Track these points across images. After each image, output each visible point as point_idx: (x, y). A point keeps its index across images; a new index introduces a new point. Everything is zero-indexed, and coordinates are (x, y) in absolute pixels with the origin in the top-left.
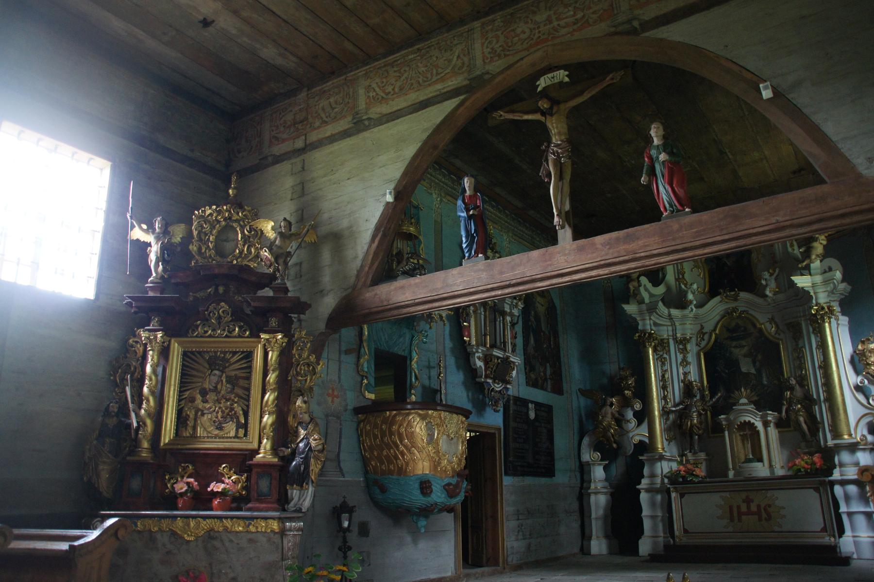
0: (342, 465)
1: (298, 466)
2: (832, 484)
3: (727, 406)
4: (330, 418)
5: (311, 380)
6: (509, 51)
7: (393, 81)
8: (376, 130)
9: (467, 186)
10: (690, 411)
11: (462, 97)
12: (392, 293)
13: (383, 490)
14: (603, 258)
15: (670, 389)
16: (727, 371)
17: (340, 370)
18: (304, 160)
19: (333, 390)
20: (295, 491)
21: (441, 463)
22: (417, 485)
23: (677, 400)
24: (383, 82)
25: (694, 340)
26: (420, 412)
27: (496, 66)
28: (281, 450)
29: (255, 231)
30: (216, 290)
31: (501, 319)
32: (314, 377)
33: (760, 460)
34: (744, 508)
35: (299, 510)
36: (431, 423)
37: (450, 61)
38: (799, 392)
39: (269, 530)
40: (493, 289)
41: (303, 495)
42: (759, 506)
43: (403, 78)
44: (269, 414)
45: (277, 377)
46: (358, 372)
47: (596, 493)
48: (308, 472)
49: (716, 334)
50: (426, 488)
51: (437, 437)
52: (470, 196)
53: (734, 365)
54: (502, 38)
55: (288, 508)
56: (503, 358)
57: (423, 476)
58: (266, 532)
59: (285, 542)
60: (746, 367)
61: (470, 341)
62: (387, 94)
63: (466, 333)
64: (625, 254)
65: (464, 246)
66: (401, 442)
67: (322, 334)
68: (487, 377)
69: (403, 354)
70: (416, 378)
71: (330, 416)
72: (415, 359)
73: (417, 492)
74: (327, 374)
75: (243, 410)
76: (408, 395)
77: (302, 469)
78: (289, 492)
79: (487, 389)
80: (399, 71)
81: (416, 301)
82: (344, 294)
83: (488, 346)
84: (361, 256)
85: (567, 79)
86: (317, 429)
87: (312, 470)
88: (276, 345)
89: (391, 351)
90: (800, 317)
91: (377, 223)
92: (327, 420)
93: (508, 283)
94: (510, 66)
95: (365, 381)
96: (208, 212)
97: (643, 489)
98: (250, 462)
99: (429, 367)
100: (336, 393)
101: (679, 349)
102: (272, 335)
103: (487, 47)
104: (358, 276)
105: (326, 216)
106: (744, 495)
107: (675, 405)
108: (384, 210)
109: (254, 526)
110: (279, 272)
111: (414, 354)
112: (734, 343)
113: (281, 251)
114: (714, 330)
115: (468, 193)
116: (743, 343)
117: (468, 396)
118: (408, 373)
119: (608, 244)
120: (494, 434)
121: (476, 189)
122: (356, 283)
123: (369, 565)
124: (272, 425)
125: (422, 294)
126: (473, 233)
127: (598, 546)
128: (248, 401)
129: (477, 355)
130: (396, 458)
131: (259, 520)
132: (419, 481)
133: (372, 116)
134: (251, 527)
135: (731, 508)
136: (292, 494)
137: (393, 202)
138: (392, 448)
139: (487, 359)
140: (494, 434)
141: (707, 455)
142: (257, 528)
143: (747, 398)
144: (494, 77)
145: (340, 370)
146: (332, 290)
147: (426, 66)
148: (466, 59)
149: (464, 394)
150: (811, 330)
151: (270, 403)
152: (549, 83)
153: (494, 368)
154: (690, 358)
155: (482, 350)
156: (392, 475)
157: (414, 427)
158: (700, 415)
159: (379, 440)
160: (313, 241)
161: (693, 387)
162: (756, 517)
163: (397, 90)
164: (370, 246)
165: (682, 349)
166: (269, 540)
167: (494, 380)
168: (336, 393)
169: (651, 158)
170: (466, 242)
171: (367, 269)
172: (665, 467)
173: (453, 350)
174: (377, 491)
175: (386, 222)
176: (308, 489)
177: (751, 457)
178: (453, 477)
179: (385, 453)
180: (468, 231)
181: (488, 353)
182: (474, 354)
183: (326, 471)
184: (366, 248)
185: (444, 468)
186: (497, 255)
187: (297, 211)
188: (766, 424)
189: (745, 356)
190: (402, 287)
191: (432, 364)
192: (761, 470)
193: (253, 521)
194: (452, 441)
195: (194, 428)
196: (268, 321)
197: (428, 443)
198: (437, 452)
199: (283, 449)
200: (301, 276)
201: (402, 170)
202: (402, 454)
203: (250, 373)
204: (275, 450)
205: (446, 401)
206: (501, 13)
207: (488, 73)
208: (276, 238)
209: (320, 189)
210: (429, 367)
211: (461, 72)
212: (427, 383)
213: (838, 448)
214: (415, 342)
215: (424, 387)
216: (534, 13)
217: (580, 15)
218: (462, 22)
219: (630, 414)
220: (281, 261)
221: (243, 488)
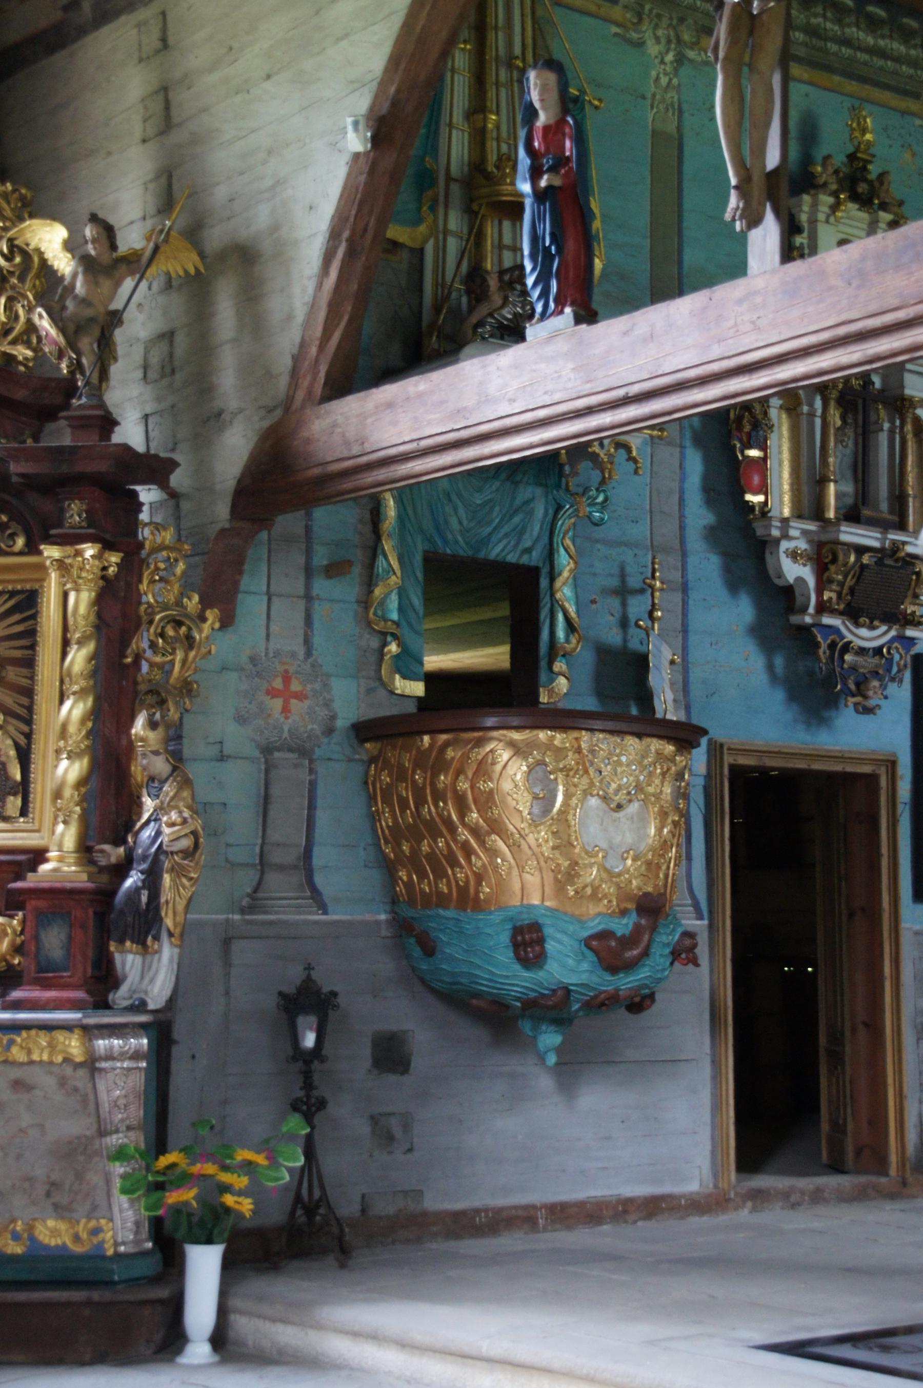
0: (319, 880)
1: (135, 891)
4: (277, 755)
5: (184, 662)
9: (535, 96)
12: (369, 421)
13: (429, 948)
14: (844, 317)
17: (308, 620)
18: (164, 14)
19: (287, 679)
20: (130, 957)
21: (578, 875)
22: (505, 937)
26: (516, 736)
28: (102, 851)
29: (26, 255)
31: (898, 423)
32: (192, 654)
35: (140, 1007)
36: (546, 765)
39: (60, 1059)
40: (589, 411)
41: (150, 967)
44: (69, 758)
45: (93, 657)
46: (369, 624)
48: (157, 909)
50: (532, 943)
51: (565, 803)
52: (546, 129)
55: (114, 1003)
56: (881, 550)
57: (521, 913)
58: (51, 1063)
59: (101, 1086)
61: (766, 503)
63: (756, 479)
64: (895, 302)
65: (530, 281)
66: (462, 815)
67: (223, 531)
68: (822, 608)
69: (525, 560)
70: (571, 627)
71: (278, 749)
72: (566, 574)
73: (505, 956)
75: (17, 746)
76: (543, 676)
77: (144, 898)
78: (118, 957)
79: (824, 646)
81: (424, 443)
82: (266, 424)
83: (831, 514)
84: (300, 315)
86: (186, 794)
87: (167, 902)
88: (84, 574)
89: (482, 555)
91: (333, 217)
92: (266, 762)
93: (621, 393)
95: (393, 648)
98: (19, 885)
99: (623, 592)
100: (295, 686)
102: (69, 550)
104: (295, 372)
105: (221, 193)
108: (349, 175)
109: (21, 1047)
110: (83, 373)
111: (562, 559)
113: (89, 312)
115: (542, 119)
117: (770, 668)
118: (544, 613)
120: (872, 779)
122: (291, 393)
123: (410, 1150)
124: (81, 783)
126: (547, 244)
128: (29, 722)
129: (784, 545)
130: (453, 862)
131: (33, 1032)
132: (509, 926)
134: (15, 1050)
136: (124, 964)
137: (366, 153)
138: (442, 836)
140: (872, 779)
142: (29, 1052)
145: (308, 620)
146: (241, 411)
149: (757, 661)
151: (72, 729)
153: (850, 582)
155: (805, 533)
156: (446, 908)
157: (496, 776)
159: (411, 812)
160: (192, 271)
164: (320, 286)
166: (62, 1082)
167: (853, 614)
168: (295, 686)
170: (533, 270)
171: (314, 350)
173: (712, 535)
174: (417, 952)
175: (353, 212)
176: (158, 952)
178: (623, 913)
179: (425, 848)
180: (535, 239)
181: (824, 538)
182: (777, 542)
185: (589, 891)
186: (885, 217)
187: (157, 177)
190: (390, 405)
191: (634, 582)
193: (19, 1035)
194: (621, 814)
196: (62, 511)
197: (535, 824)
198: (564, 845)
199: (106, 847)
200: (173, 372)
201: (386, 49)
202: (468, 851)
203: (33, 647)
204: (85, 850)
205: (684, 688)
208: (75, 275)
209: (205, 110)
210: (623, 592)
212: (613, 637)
214: (564, 523)
215: (604, 653)
220: (87, 343)
221: (18, 949)
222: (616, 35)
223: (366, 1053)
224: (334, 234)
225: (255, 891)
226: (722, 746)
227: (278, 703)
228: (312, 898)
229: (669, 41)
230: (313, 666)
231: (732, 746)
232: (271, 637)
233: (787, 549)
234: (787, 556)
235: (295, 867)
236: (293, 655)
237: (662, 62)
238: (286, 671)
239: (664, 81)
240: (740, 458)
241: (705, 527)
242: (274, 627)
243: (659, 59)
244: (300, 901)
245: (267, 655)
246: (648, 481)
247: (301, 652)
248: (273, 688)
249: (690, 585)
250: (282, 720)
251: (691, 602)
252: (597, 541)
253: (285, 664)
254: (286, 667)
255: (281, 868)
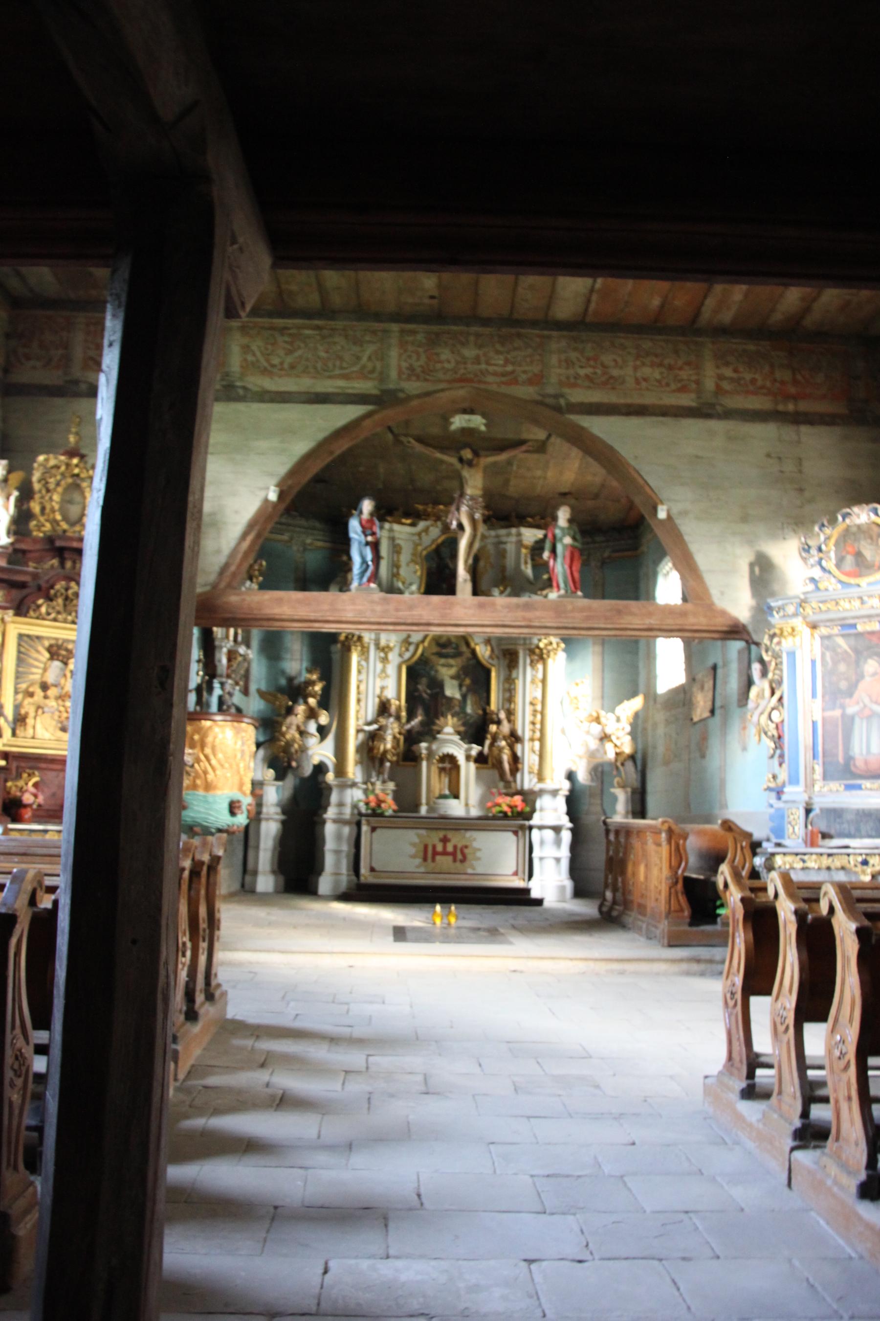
2: (531, 828)
3: (429, 731)
6: (429, 375)
7: (281, 353)
8: (255, 406)
10: (385, 732)
11: (370, 408)
15: (363, 704)
16: (429, 691)
23: (370, 717)
24: (267, 349)
25: (396, 651)
27: (413, 387)
30: (62, 564)
33: (457, 797)
34: (440, 848)
37: (358, 358)
38: (506, 728)
42: (455, 847)
43: (297, 354)
47: (267, 819)
49: (424, 647)
53: (437, 685)
54: (423, 358)
60: (452, 691)
62: (273, 366)
73: (226, 811)
80: (291, 343)
85: (483, 428)
90: (520, 645)
94: (428, 394)
96: (52, 462)
97: (330, 819)
101: (380, 657)
103: (405, 361)
106: (441, 834)
107: (369, 724)
112: (442, 661)
114: (423, 641)
116: (451, 661)
119: (509, 607)
121: (372, 514)
125: (302, 612)
127: (265, 882)
133: (250, 386)
135: (426, 847)
137: (273, 503)
139: (231, 655)
141: (397, 785)
143: (454, 727)
144: (409, 398)
147: (327, 352)
148: (378, 365)
150: (528, 661)
152: (465, 425)
154: (391, 669)
158: (395, 737)
161: (390, 705)
162: (450, 858)
163: (286, 366)
165: (383, 659)
169: (554, 537)
172: (356, 795)
177: (447, 792)
184: (233, 544)
188: (468, 758)
189: (453, 677)
192: (455, 808)
195: (34, 727)
206: (425, 327)
207: (402, 390)
211: (370, 376)
213: (541, 792)
216: (463, 344)
217: (509, 368)
218: (378, 317)
219: (312, 727)
224: (251, 526)
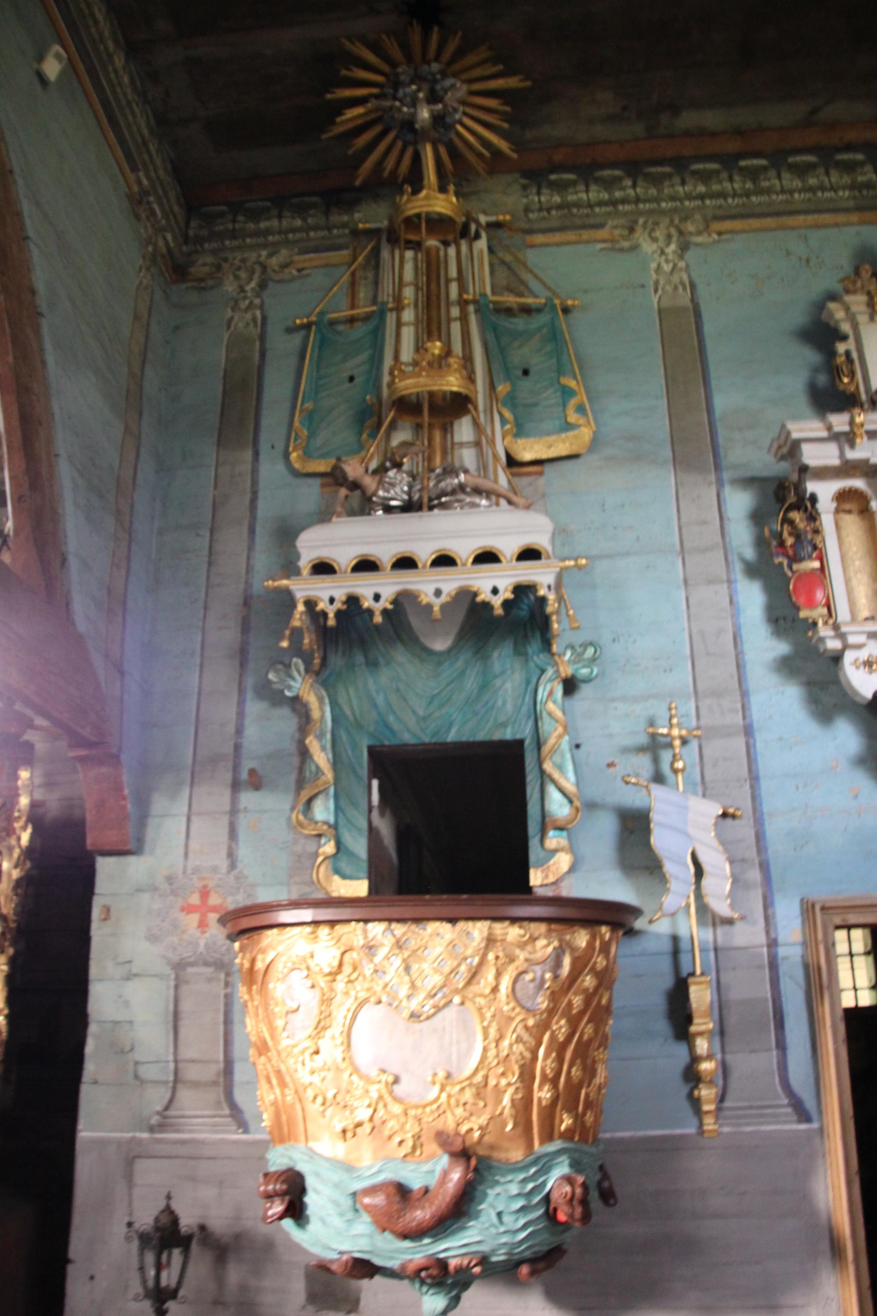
19: (205, 894)
63: (819, 595)
71: (192, 965)
74: (186, 855)
92: (177, 978)
129: (849, 657)
183: (183, 1117)
222: (602, 250)
223: (298, 1289)
225: (167, 1108)
226: (813, 906)
227: (195, 918)
228: (231, 1116)
229: (669, 237)
230: (237, 878)
231: (828, 904)
232: (191, 856)
233: (856, 660)
234: (858, 668)
235: (215, 1083)
236: (215, 869)
237: (663, 252)
238: (205, 887)
239: (667, 268)
240: (789, 574)
241: (775, 660)
242: (193, 845)
243: (659, 252)
244: (216, 1119)
245: (184, 872)
246: (686, 625)
247: (224, 864)
248: (189, 905)
249: (755, 725)
250: (199, 934)
251: (759, 745)
252: (613, 700)
253: (204, 879)
254: (205, 882)
255: (196, 1085)
